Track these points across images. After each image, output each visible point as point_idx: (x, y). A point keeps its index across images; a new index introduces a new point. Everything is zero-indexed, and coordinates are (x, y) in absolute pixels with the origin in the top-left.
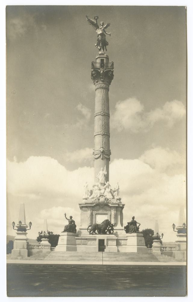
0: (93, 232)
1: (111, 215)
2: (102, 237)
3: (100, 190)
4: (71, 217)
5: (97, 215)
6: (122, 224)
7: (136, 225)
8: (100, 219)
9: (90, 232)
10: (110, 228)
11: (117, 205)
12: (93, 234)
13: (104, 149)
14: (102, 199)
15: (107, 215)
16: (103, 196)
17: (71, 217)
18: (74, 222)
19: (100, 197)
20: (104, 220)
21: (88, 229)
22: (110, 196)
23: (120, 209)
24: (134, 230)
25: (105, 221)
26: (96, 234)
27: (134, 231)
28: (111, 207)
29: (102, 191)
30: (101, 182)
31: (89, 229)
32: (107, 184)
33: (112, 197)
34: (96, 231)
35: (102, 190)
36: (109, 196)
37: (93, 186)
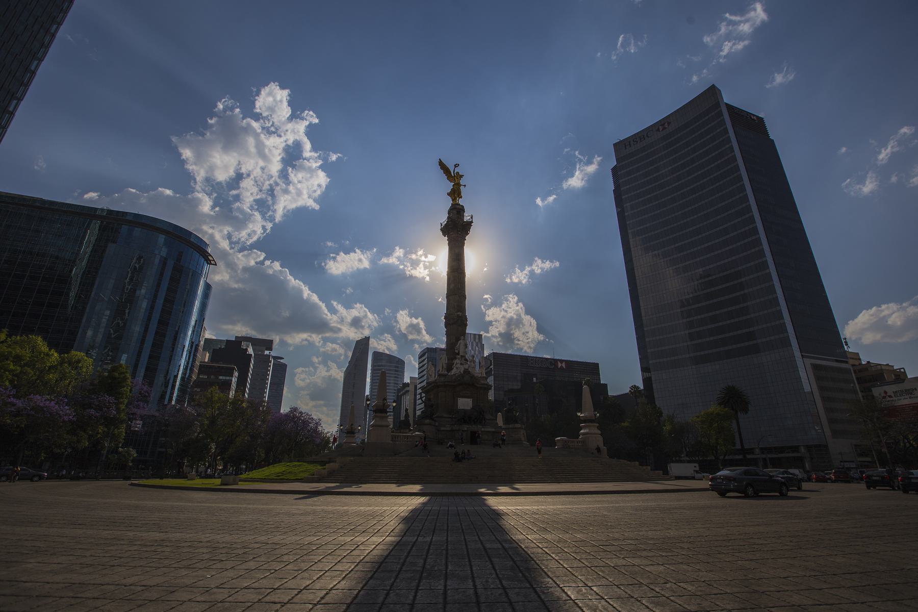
2: (474, 428)
29: (466, 367)
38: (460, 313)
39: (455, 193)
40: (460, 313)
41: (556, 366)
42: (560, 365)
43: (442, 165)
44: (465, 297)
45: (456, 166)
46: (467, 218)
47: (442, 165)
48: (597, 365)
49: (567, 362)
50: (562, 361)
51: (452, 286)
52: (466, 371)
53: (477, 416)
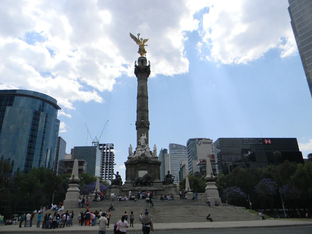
0: (136, 185)
1: (150, 171)
3: (141, 150)
4: (118, 173)
5: (139, 171)
6: (160, 179)
7: (171, 178)
8: (142, 174)
9: (133, 185)
10: (150, 181)
11: (155, 162)
12: (135, 187)
13: (145, 120)
14: (143, 158)
15: (147, 171)
16: (143, 155)
17: (118, 173)
18: (120, 176)
19: (141, 156)
20: (144, 174)
21: (131, 183)
22: (149, 155)
23: (158, 165)
24: (169, 182)
25: (146, 175)
26: (138, 186)
27: (170, 183)
28: (150, 164)
29: (143, 152)
30: (142, 145)
31: (133, 183)
32: (147, 146)
33: (151, 156)
34: (139, 184)
35: (143, 151)
36: (149, 156)
37: (136, 149)
38: (143, 121)
39: (142, 51)
40: (143, 121)
41: (264, 143)
42: (266, 142)
43: (132, 37)
44: (147, 111)
45: (139, 35)
46: (147, 65)
47: (132, 37)
48: (296, 138)
49: (271, 139)
50: (268, 139)
51: (139, 105)
52: (143, 155)
53: (147, 181)
